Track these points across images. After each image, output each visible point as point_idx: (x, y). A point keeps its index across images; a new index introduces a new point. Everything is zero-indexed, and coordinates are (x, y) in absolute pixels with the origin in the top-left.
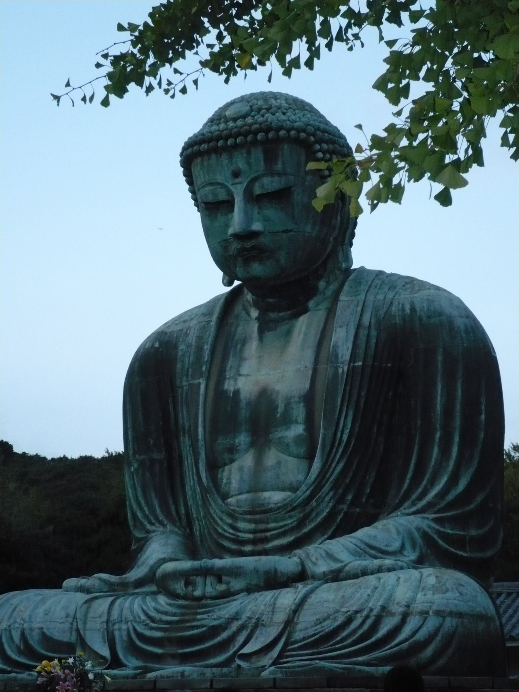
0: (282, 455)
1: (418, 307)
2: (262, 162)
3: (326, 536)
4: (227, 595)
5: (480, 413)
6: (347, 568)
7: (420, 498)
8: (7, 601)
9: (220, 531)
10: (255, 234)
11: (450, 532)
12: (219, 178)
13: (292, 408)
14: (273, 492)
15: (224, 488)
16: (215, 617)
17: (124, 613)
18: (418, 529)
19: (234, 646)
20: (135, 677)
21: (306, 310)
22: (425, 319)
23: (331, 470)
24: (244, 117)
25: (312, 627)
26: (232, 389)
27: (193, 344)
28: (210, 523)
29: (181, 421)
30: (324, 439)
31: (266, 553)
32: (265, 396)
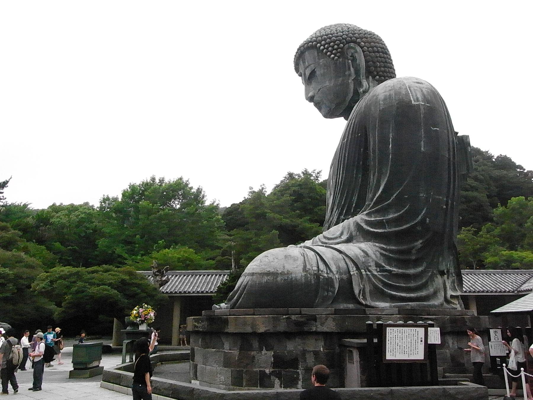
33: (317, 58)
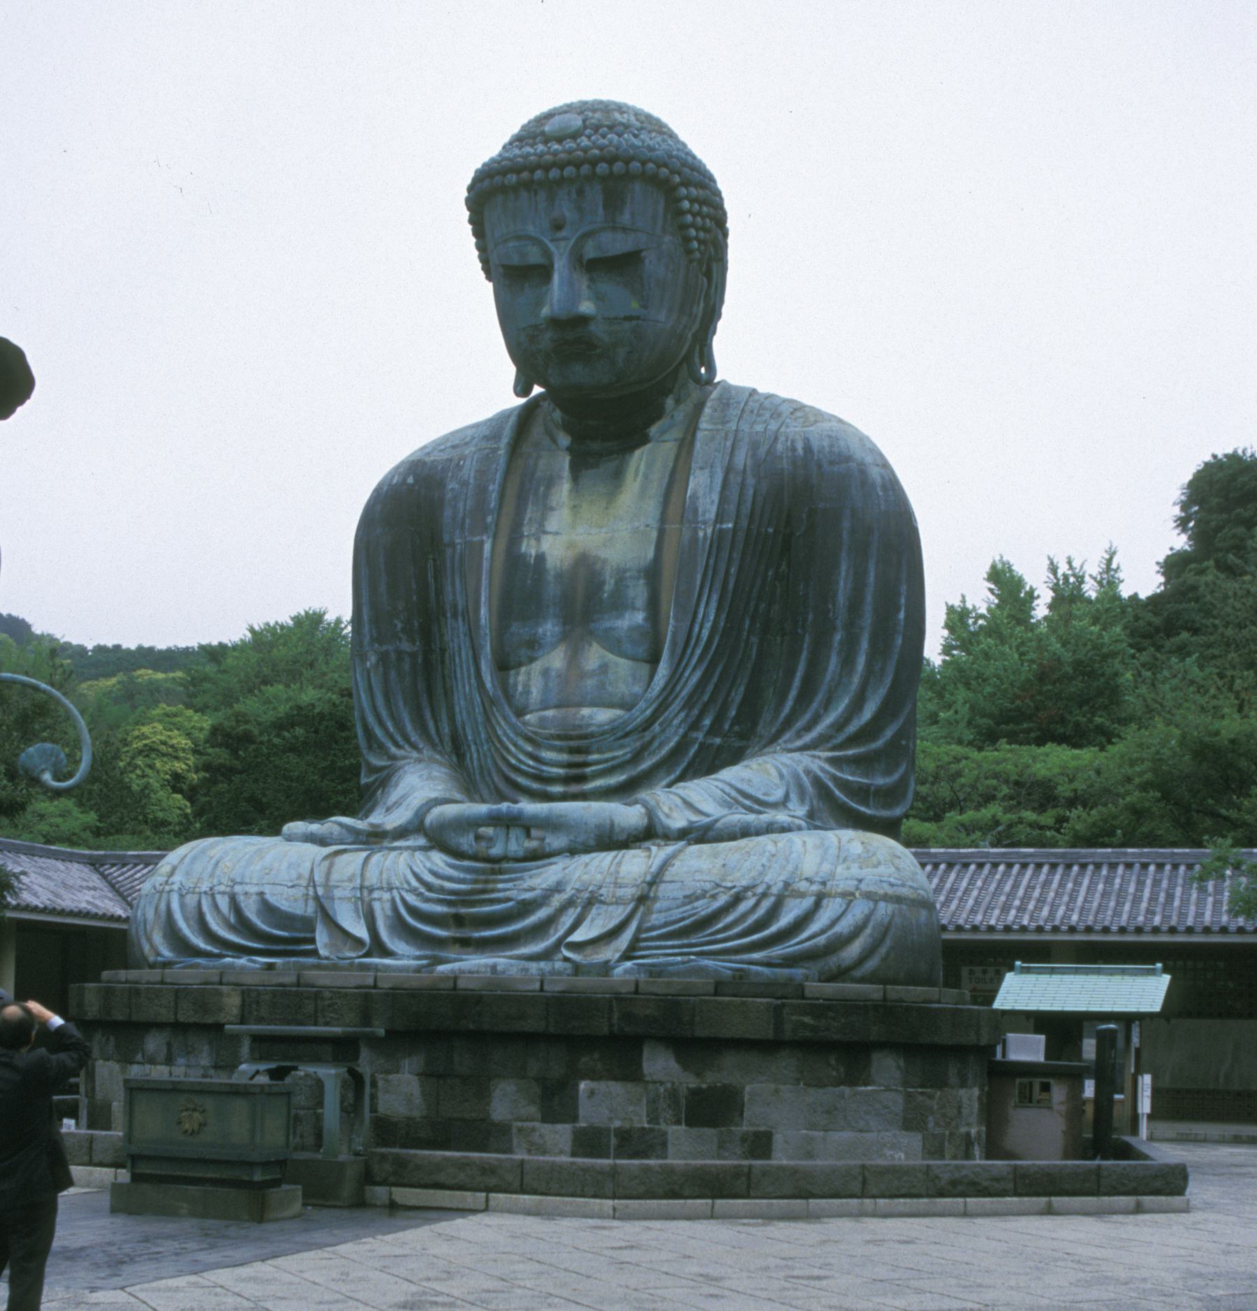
0: (611, 657)
1: (815, 444)
2: (601, 209)
3: (672, 777)
4: (538, 856)
5: (898, 610)
6: (719, 825)
7: (808, 728)
8: (203, 852)
9: (513, 761)
10: (583, 320)
11: (850, 778)
12: (531, 230)
13: (627, 587)
14: (595, 709)
15: (519, 700)
16: (525, 886)
17: (384, 876)
18: (808, 772)
19: (556, 931)
20: (418, 970)
21: (645, 440)
22: (825, 465)
23: (684, 680)
24: (575, 136)
25: (678, 907)
26: (533, 552)
27: (472, 481)
28: (497, 750)
29: (449, 598)
30: (674, 634)
31: (583, 796)
32: (585, 566)
33: (660, 223)
